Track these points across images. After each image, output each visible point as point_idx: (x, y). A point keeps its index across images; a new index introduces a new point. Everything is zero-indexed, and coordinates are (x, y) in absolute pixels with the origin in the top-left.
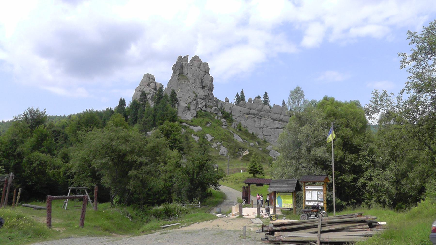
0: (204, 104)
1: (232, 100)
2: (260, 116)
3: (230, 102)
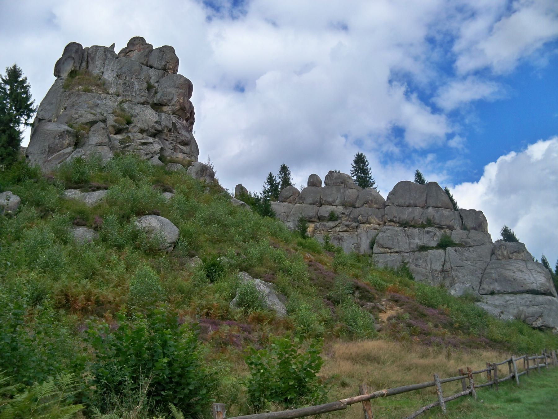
0: (157, 147)
2: (355, 220)
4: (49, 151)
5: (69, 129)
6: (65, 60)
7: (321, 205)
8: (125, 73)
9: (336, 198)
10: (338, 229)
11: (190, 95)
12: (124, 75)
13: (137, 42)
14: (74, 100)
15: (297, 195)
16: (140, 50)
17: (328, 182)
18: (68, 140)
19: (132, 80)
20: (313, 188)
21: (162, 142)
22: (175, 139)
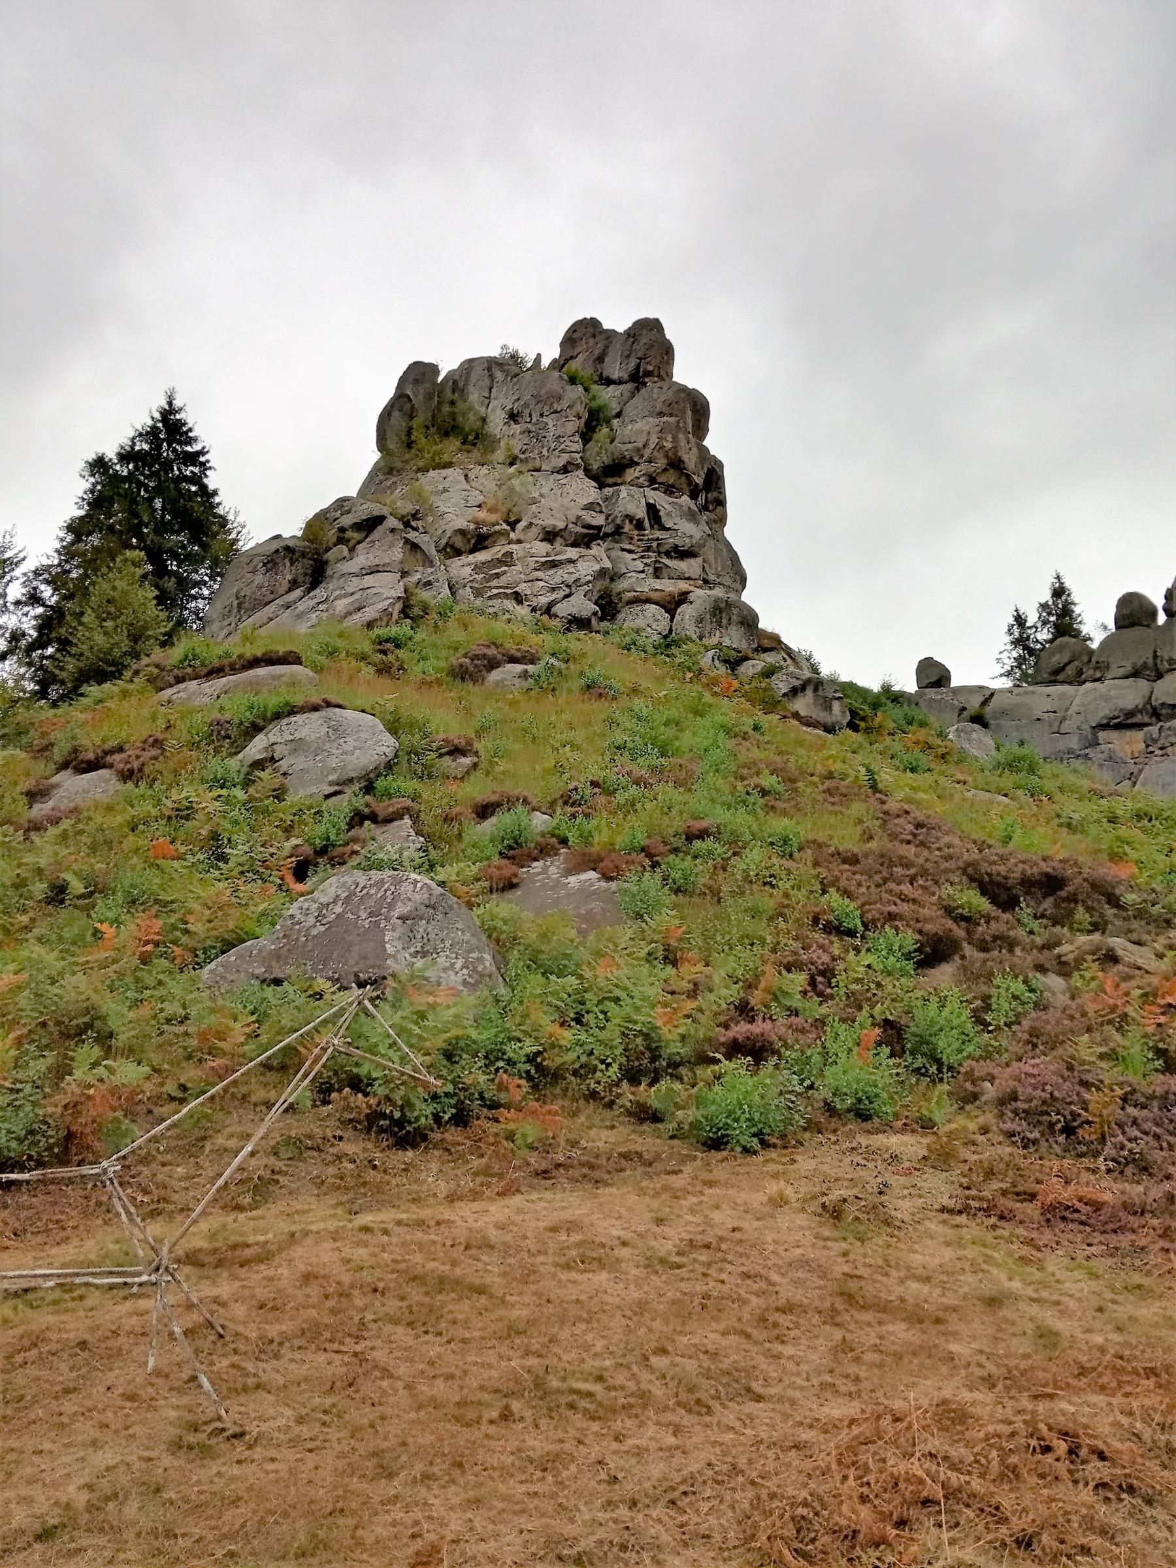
7: (1160, 676)
8: (526, 405)
12: (526, 412)
15: (1085, 659)
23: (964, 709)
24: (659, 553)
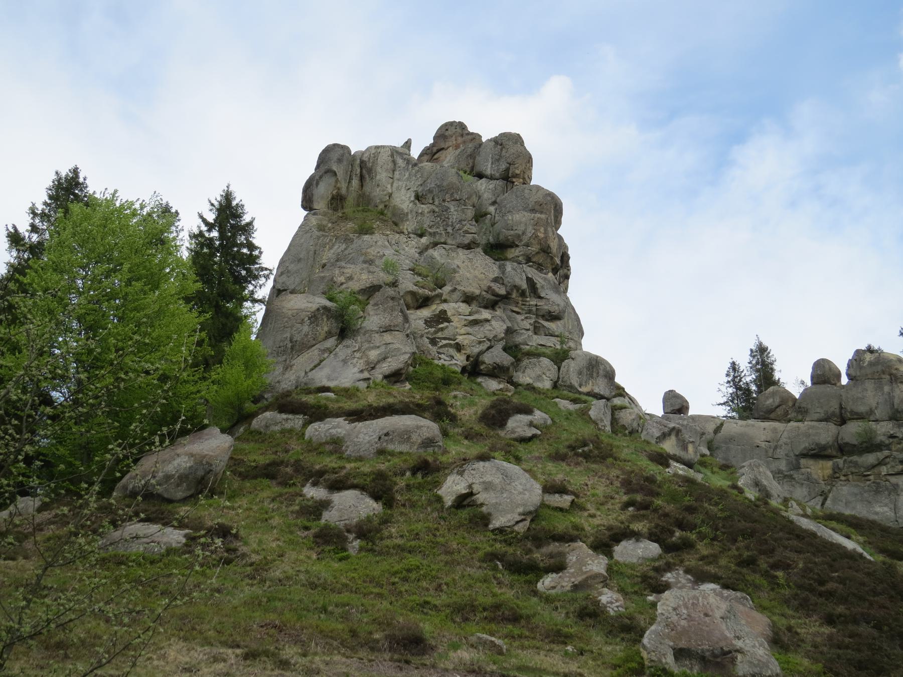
0: (498, 327)
1: (709, 401)
3: (691, 412)
4: (292, 348)
5: (328, 304)
6: (321, 177)
7: (843, 421)
8: (430, 191)
9: (874, 405)
10: (884, 470)
11: (558, 223)
12: (430, 196)
13: (452, 134)
14: (339, 250)
15: (790, 404)
16: (457, 147)
17: (853, 374)
18: (325, 326)
19: (446, 204)
20: (822, 388)
21: (509, 318)
22: (534, 309)
23: (703, 434)
24: (537, 316)
